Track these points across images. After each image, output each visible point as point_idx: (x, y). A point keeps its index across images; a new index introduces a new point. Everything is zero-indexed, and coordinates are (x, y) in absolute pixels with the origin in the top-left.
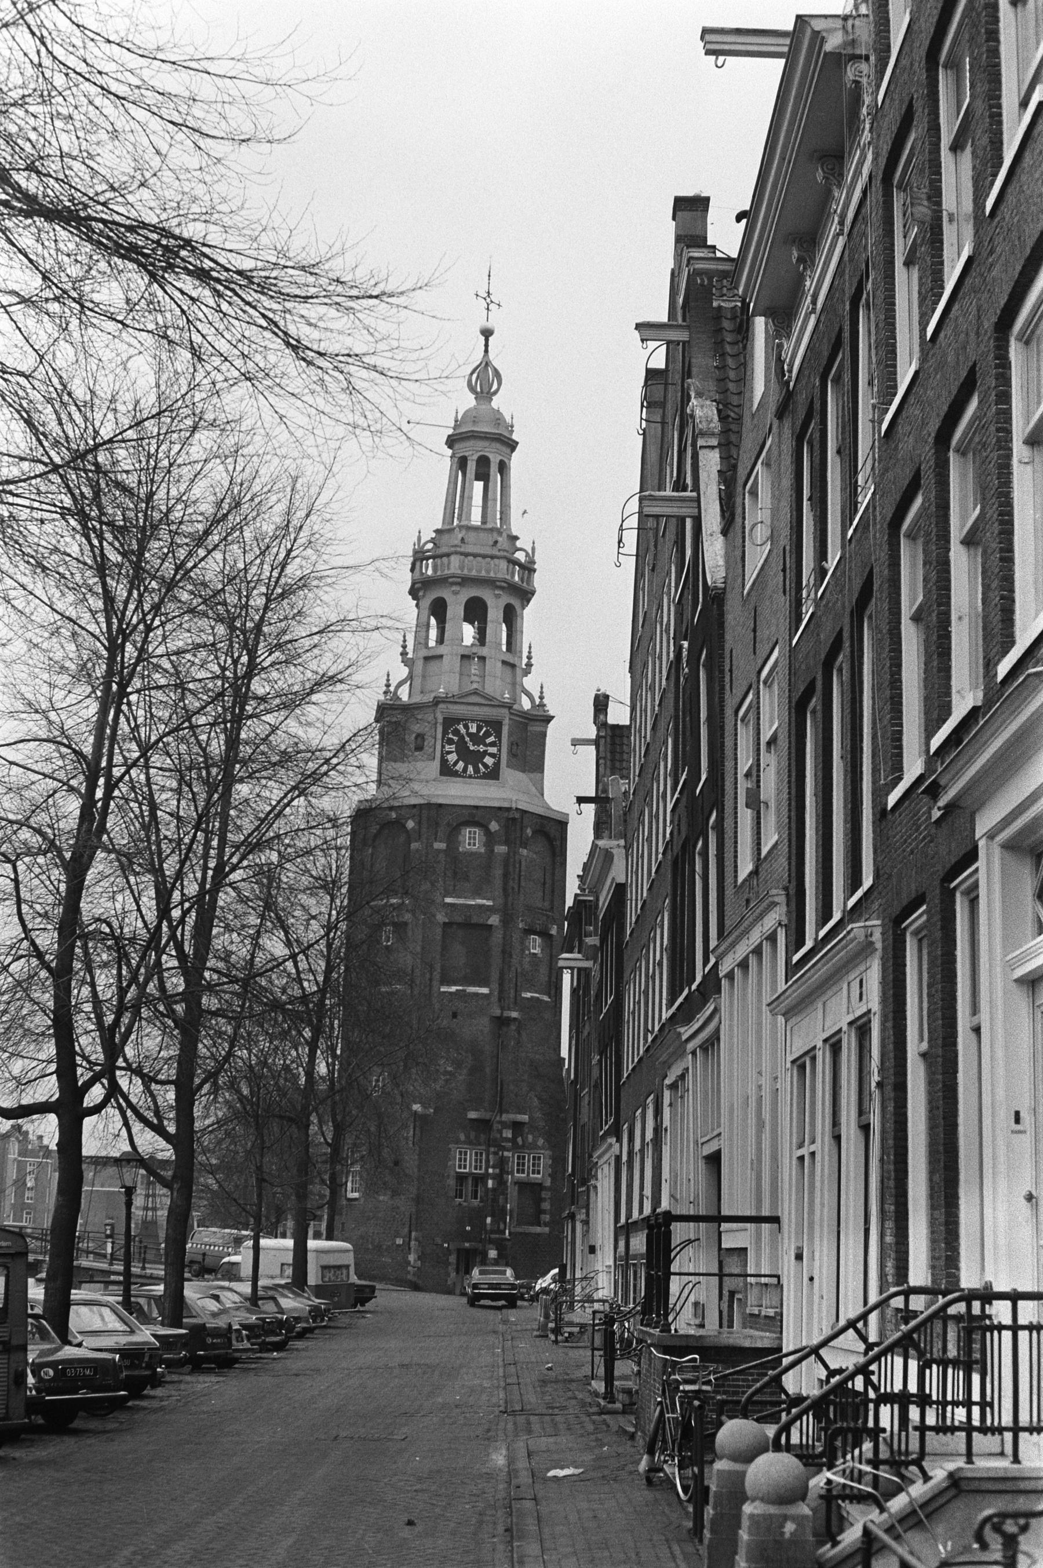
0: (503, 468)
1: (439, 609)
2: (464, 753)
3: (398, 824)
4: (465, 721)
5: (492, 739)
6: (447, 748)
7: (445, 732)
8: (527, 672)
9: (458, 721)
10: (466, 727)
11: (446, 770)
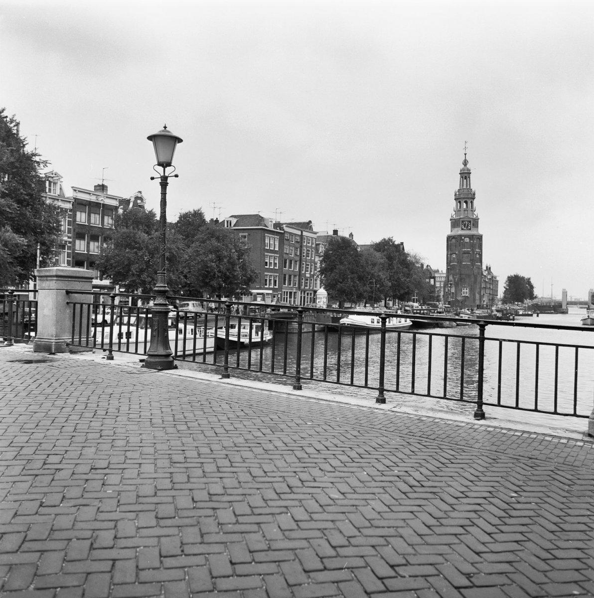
0: (469, 177)
11: (462, 229)
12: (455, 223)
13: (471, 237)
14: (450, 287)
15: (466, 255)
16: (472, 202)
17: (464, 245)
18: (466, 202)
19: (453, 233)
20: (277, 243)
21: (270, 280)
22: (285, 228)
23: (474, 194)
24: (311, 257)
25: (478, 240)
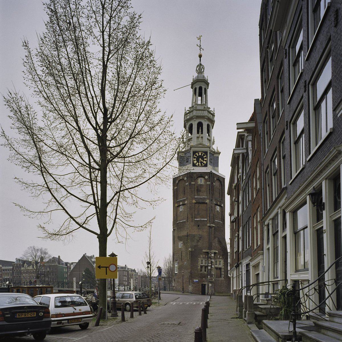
1: (191, 126)
2: (198, 161)
3: (183, 179)
4: (198, 152)
5: (205, 156)
6: (194, 159)
7: (193, 156)
9: (197, 152)
10: (199, 154)
23: (213, 115)
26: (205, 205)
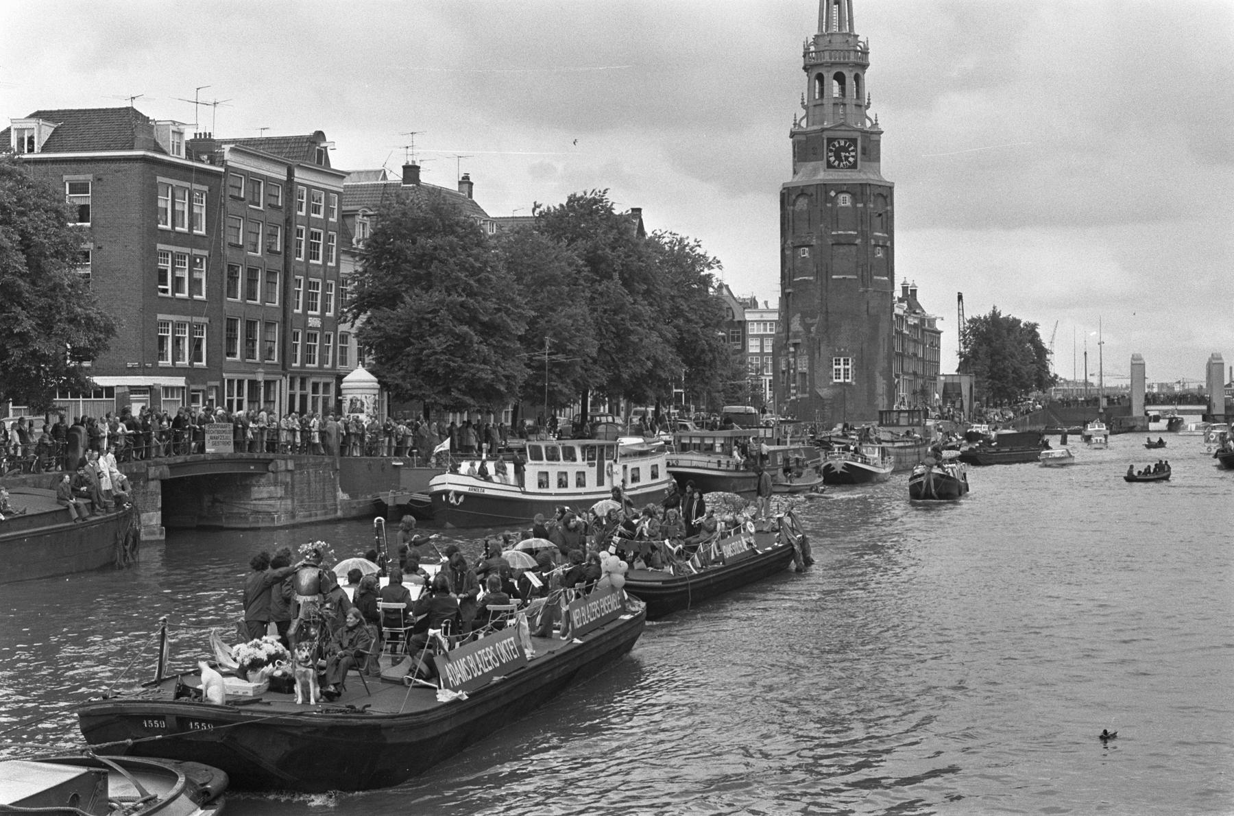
2: (838, 158)
8: (868, 107)
9: (835, 139)
12: (806, 147)
13: (859, 191)
14: (794, 355)
15: (842, 250)
16: (857, 78)
17: (835, 218)
18: (840, 78)
19: (801, 180)
20: (201, 210)
21: (177, 342)
22: (227, 156)
23: (865, 52)
24: (327, 258)
25: (880, 199)
26: (853, 248)
